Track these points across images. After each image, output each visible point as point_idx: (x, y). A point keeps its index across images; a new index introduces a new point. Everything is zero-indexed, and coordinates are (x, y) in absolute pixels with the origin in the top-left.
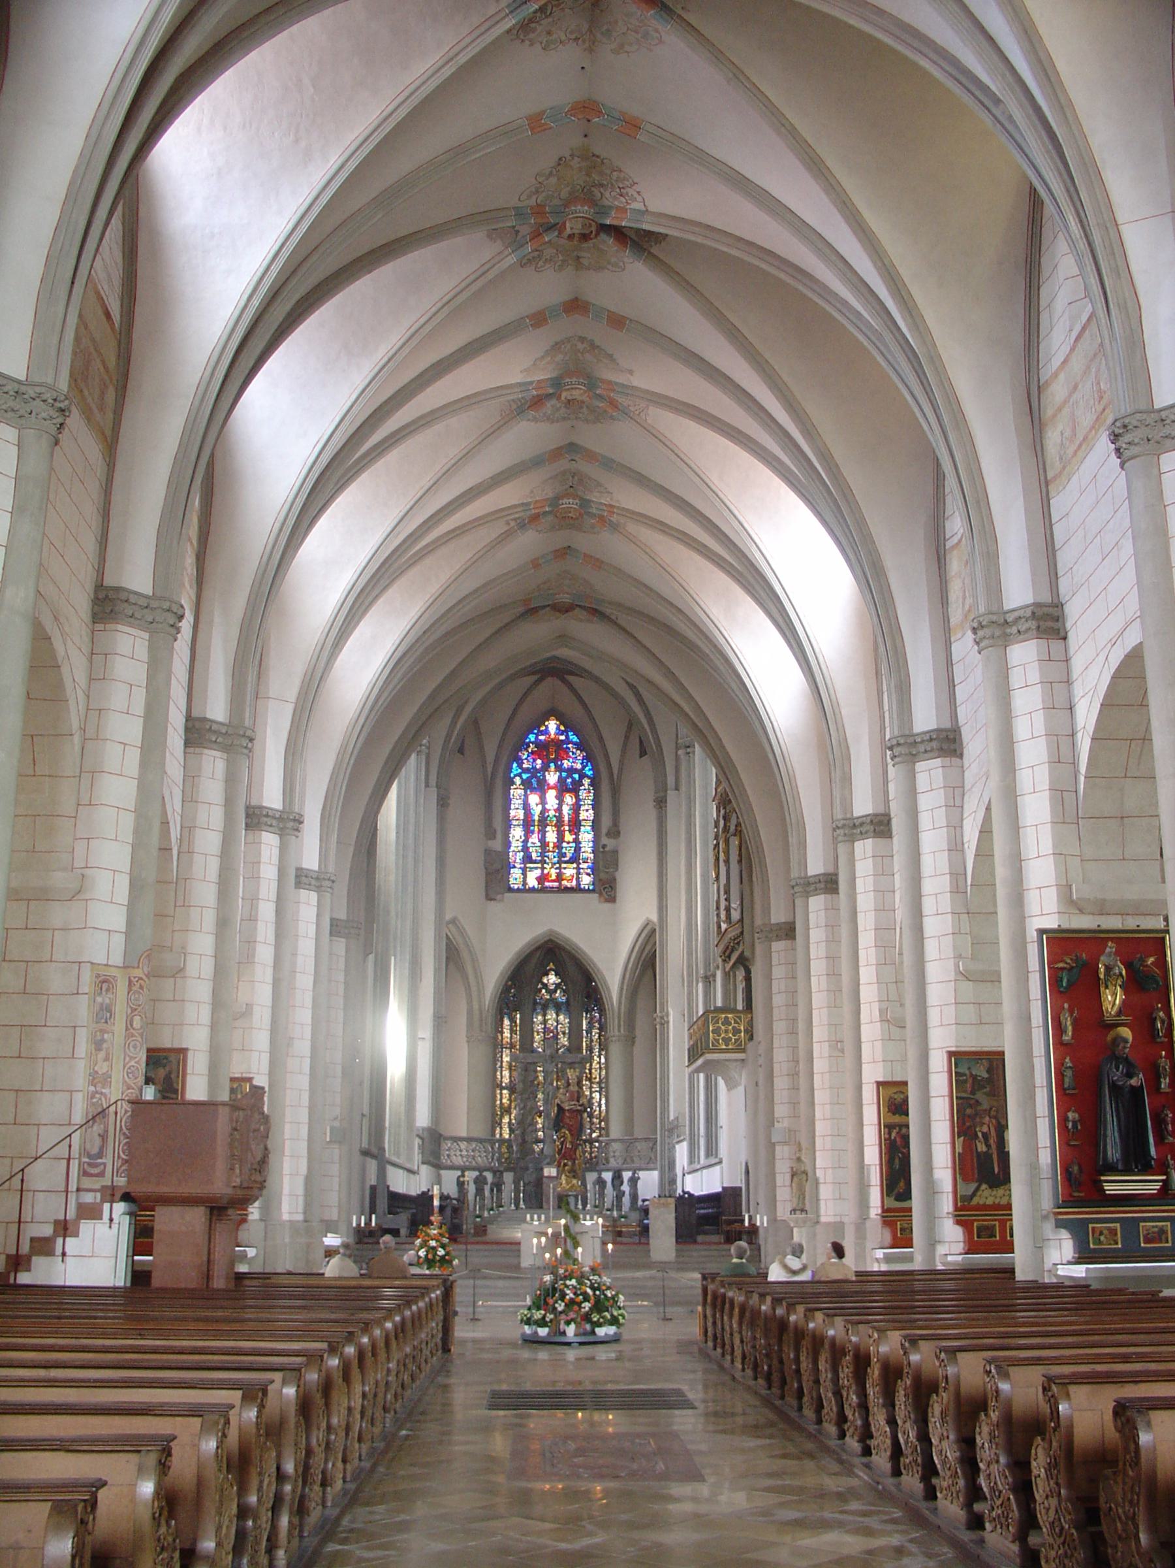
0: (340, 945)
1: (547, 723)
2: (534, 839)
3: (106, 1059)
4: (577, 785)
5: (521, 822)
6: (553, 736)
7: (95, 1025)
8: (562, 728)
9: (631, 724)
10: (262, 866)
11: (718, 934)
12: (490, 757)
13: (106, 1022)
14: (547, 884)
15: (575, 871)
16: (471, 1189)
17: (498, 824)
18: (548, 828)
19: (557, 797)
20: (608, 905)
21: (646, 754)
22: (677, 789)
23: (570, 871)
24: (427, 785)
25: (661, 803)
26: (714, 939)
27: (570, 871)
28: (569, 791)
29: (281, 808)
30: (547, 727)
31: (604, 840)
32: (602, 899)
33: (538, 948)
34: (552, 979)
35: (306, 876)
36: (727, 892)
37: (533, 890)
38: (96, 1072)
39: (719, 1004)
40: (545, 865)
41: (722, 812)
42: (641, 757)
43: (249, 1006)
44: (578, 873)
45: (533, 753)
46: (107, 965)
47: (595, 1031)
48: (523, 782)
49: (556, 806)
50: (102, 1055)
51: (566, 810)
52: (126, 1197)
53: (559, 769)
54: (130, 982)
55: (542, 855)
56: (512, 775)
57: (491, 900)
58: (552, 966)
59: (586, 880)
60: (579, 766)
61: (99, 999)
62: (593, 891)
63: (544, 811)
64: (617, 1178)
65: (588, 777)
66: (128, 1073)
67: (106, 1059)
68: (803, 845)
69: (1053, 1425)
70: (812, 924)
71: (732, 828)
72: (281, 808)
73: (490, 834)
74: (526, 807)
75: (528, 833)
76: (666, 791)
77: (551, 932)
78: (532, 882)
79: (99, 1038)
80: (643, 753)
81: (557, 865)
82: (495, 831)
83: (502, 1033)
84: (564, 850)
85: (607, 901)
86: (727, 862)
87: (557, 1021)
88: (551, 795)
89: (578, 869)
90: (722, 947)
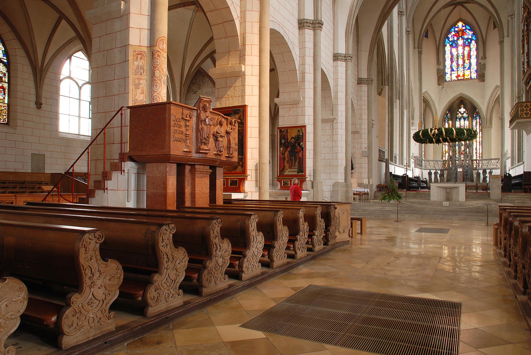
0: (365, 88)
1: (458, 24)
2: (454, 64)
3: (142, 93)
4: (469, 43)
6: (460, 28)
8: (464, 25)
9: (491, 16)
10: (306, 43)
11: (523, 74)
12: (438, 39)
13: (141, 74)
14: (459, 78)
15: (470, 73)
16: (433, 176)
20: (482, 83)
21: (496, 27)
22: (508, 36)
23: (467, 72)
24: (414, 48)
25: (501, 43)
26: (522, 76)
27: (467, 72)
29: (313, 19)
30: (458, 25)
31: (480, 61)
32: (480, 81)
33: (457, 99)
34: (462, 110)
35: (340, 56)
39: (524, 101)
41: (526, 23)
42: (494, 29)
43: (304, 98)
45: (453, 35)
46: (140, 46)
47: (478, 126)
48: (450, 46)
49: (462, 52)
50: (139, 91)
52: (131, 159)
53: (463, 39)
54: (153, 53)
55: (457, 69)
56: (446, 44)
57: (439, 85)
59: (474, 76)
61: (136, 63)
64: (484, 172)
65: (474, 40)
66: (153, 99)
67: (142, 93)
72: (313, 19)
73: (438, 63)
74: (451, 53)
76: (504, 38)
77: (461, 93)
78: (454, 78)
79: (137, 82)
80: (495, 27)
82: (441, 63)
84: (465, 66)
85: (481, 81)
88: (460, 49)
89: (471, 72)
90: (525, 79)
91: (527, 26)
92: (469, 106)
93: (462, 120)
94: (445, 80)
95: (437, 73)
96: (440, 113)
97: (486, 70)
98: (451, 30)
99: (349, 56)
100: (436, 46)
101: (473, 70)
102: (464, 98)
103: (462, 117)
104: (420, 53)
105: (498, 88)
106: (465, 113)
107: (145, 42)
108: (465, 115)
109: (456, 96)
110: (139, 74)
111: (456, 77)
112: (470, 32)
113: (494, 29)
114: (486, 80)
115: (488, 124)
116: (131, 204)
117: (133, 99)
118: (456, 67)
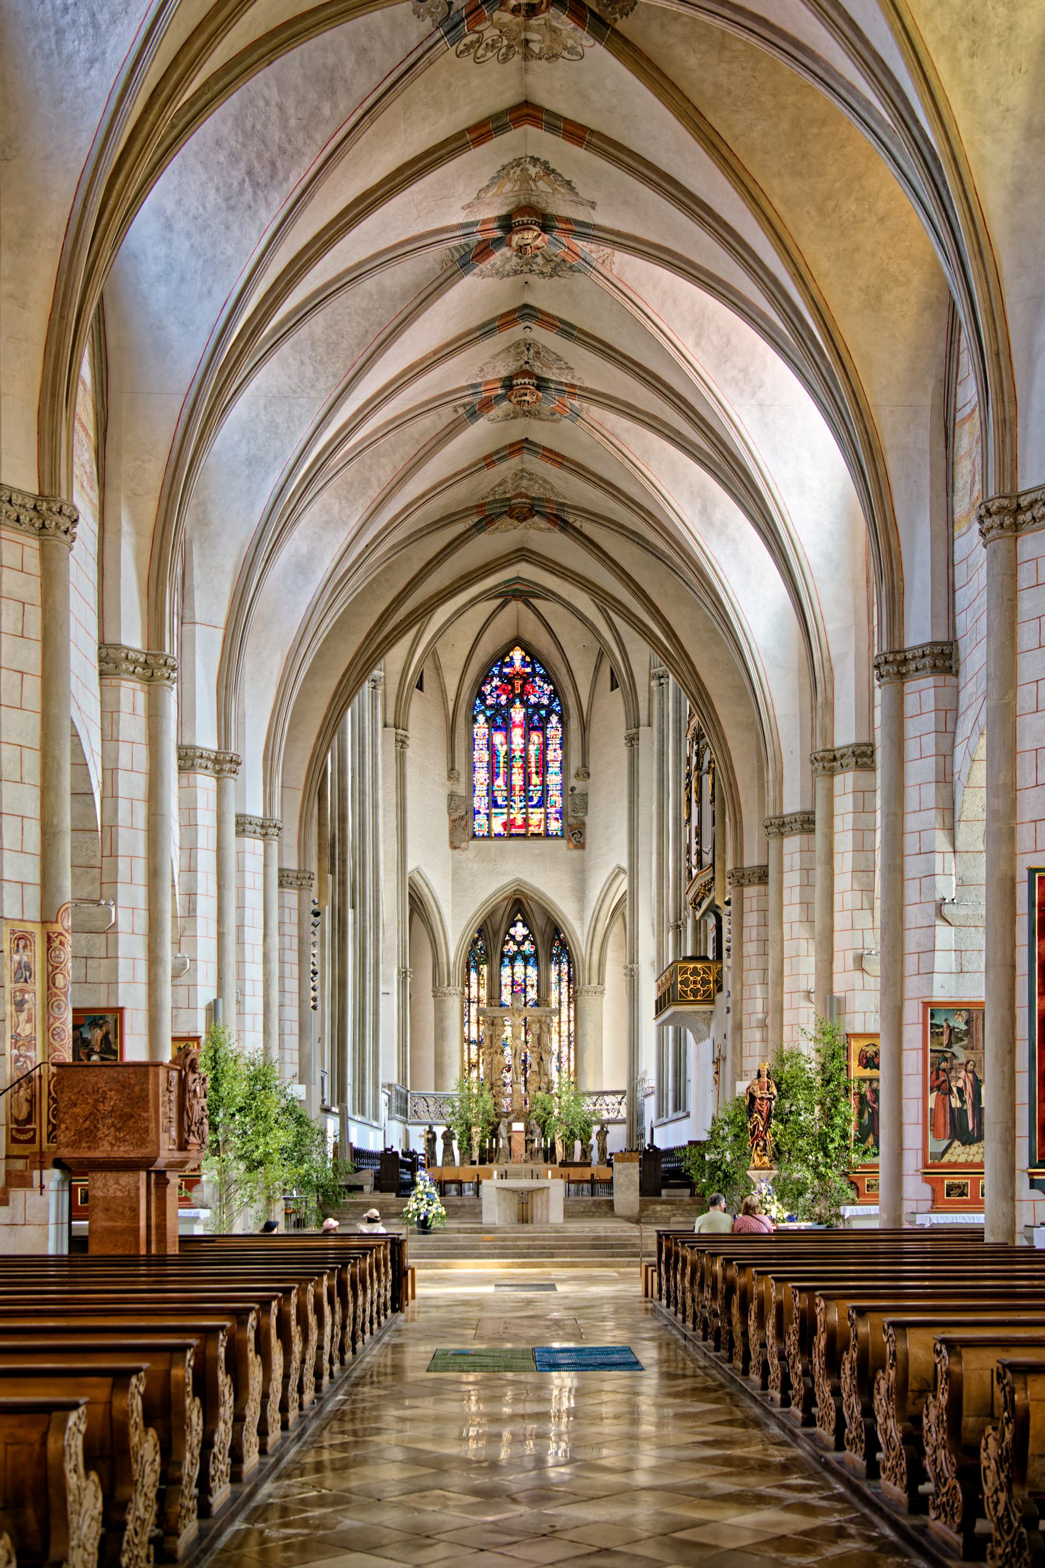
2: (500, 782)
5: (485, 765)
14: (514, 831)
15: (542, 816)
17: (461, 765)
18: (514, 770)
19: (524, 736)
20: (576, 853)
22: (649, 725)
23: (536, 816)
24: (385, 726)
25: (632, 740)
28: (535, 729)
31: (573, 782)
32: (571, 846)
35: (250, 823)
36: (699, 834)
37: (498, 835)
40: (512, 811)
41: (695, 747)
42: (612, 690)
44: (547, 818)
45: (497, 688)
46: (22, 920)
47: (564, 984)
48: (487, 721)
51: (532, 749)
53: (525, 704)
58: (519, 917)
59: (555, 826)
60: (545, 701)
61: (16, 957)
62: (562, 836)
63: (509, 753)
68: (780, 781)
69: (1006, 1414)
70: (786, 867)
71: (706, 765)
74: (491, 748)
75: (493, 775)
77: (517, 880)
78: (497, 827)
80: (614, 686)
81: (524, 810)
83: (469, 986)
84: (531, 794)
85: (576, 847)
86: (699, 802)
87: (525, 974)
88: (517, 734)
91: (697, 754)
92: (539, 921)
93: (519, 965)
94: (471, 834)
95: (449, 807)
96: (458, 937)
97: (589, 812)
98: (490, 670)
99: (275, 827)
100: (446, 716)
101: (553, 810)
102: (526, 896)
103: (519, 952)
104: (402, 743)
105: (622, 876)
106: (527, 943)
107: (33, 913)
108: (527, 947)
109: (502, 888)
111: (504, 825)
112: (546, 686)
113: (612, 690)
114: (587, 845)
115: (594, 983)
116: (51, 1251)
118: (505, 794)
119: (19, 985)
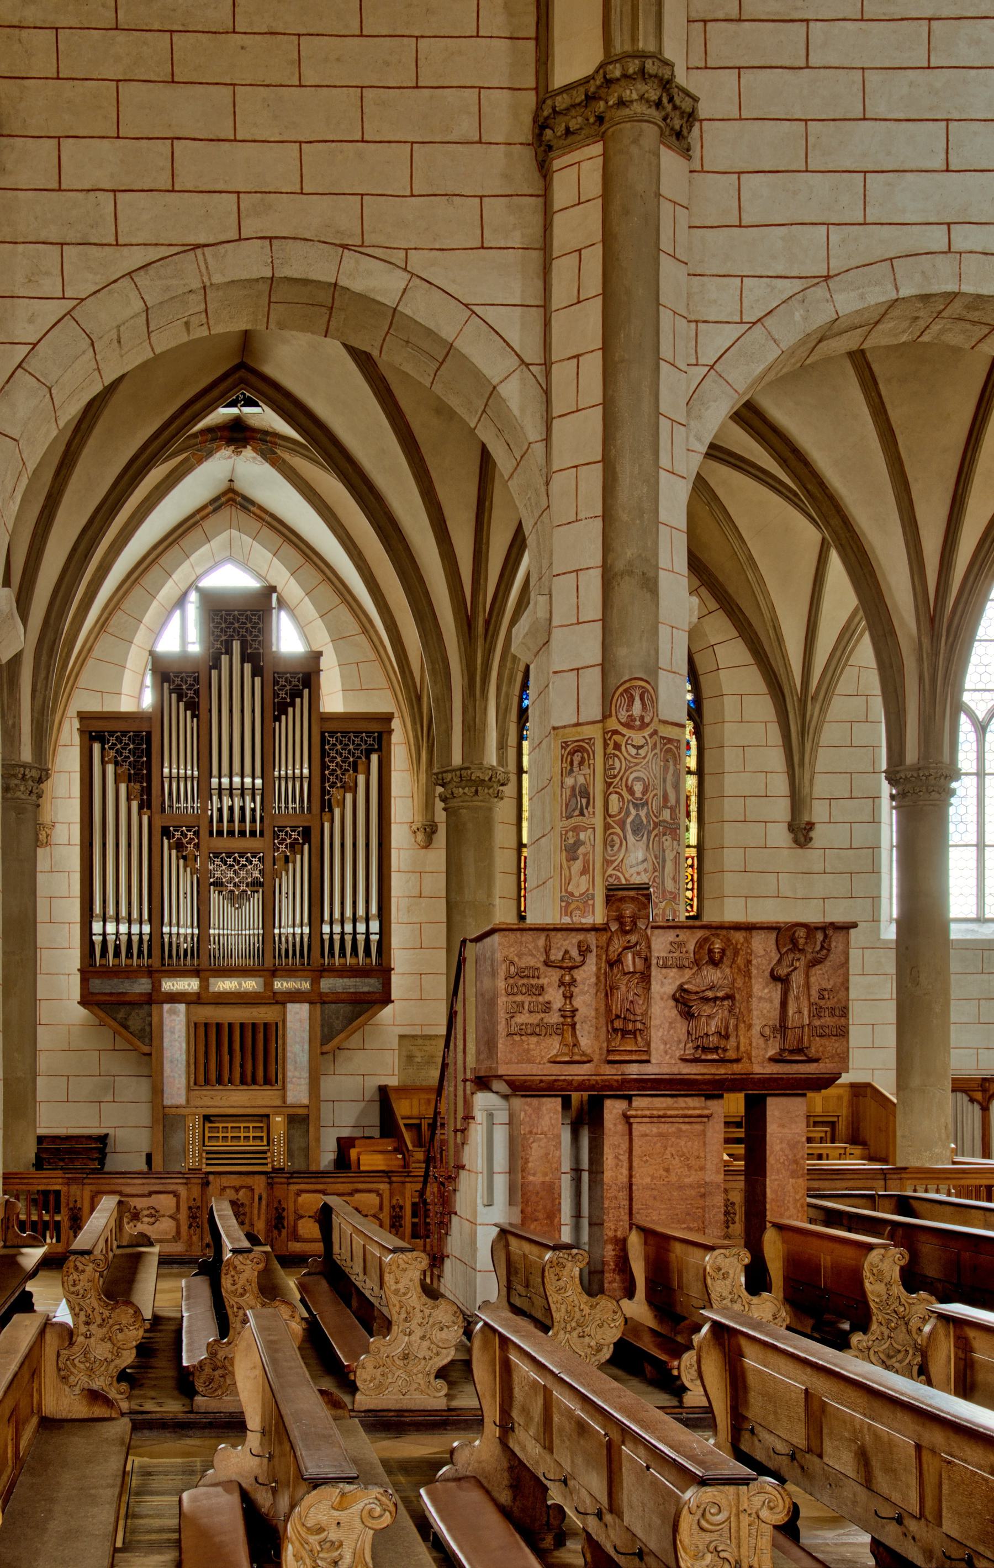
7: (566, 823)
13: (582, 814)
38: (572, 894)
46: (578, 724)
50: (577, 866)
61: (569, 781)
67: (584, 871)
79: (571, 841)
110: (577, 812)
117: (564, 894)
119: (573, 820)
